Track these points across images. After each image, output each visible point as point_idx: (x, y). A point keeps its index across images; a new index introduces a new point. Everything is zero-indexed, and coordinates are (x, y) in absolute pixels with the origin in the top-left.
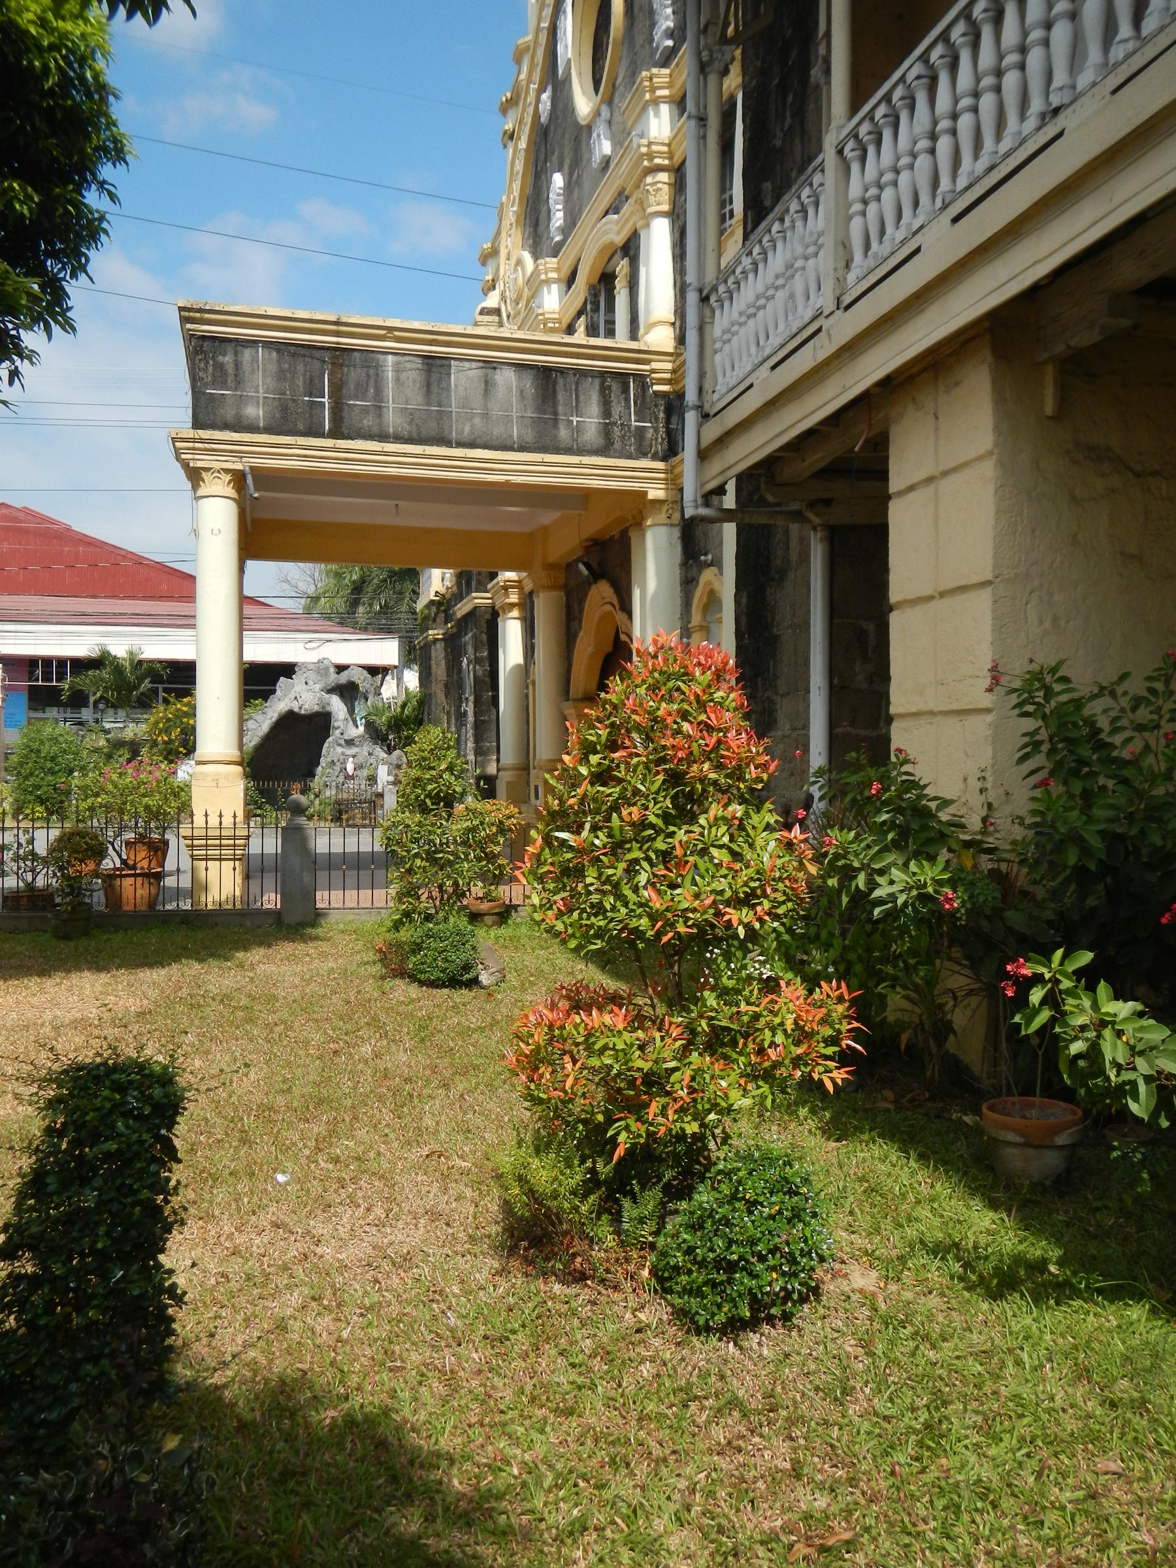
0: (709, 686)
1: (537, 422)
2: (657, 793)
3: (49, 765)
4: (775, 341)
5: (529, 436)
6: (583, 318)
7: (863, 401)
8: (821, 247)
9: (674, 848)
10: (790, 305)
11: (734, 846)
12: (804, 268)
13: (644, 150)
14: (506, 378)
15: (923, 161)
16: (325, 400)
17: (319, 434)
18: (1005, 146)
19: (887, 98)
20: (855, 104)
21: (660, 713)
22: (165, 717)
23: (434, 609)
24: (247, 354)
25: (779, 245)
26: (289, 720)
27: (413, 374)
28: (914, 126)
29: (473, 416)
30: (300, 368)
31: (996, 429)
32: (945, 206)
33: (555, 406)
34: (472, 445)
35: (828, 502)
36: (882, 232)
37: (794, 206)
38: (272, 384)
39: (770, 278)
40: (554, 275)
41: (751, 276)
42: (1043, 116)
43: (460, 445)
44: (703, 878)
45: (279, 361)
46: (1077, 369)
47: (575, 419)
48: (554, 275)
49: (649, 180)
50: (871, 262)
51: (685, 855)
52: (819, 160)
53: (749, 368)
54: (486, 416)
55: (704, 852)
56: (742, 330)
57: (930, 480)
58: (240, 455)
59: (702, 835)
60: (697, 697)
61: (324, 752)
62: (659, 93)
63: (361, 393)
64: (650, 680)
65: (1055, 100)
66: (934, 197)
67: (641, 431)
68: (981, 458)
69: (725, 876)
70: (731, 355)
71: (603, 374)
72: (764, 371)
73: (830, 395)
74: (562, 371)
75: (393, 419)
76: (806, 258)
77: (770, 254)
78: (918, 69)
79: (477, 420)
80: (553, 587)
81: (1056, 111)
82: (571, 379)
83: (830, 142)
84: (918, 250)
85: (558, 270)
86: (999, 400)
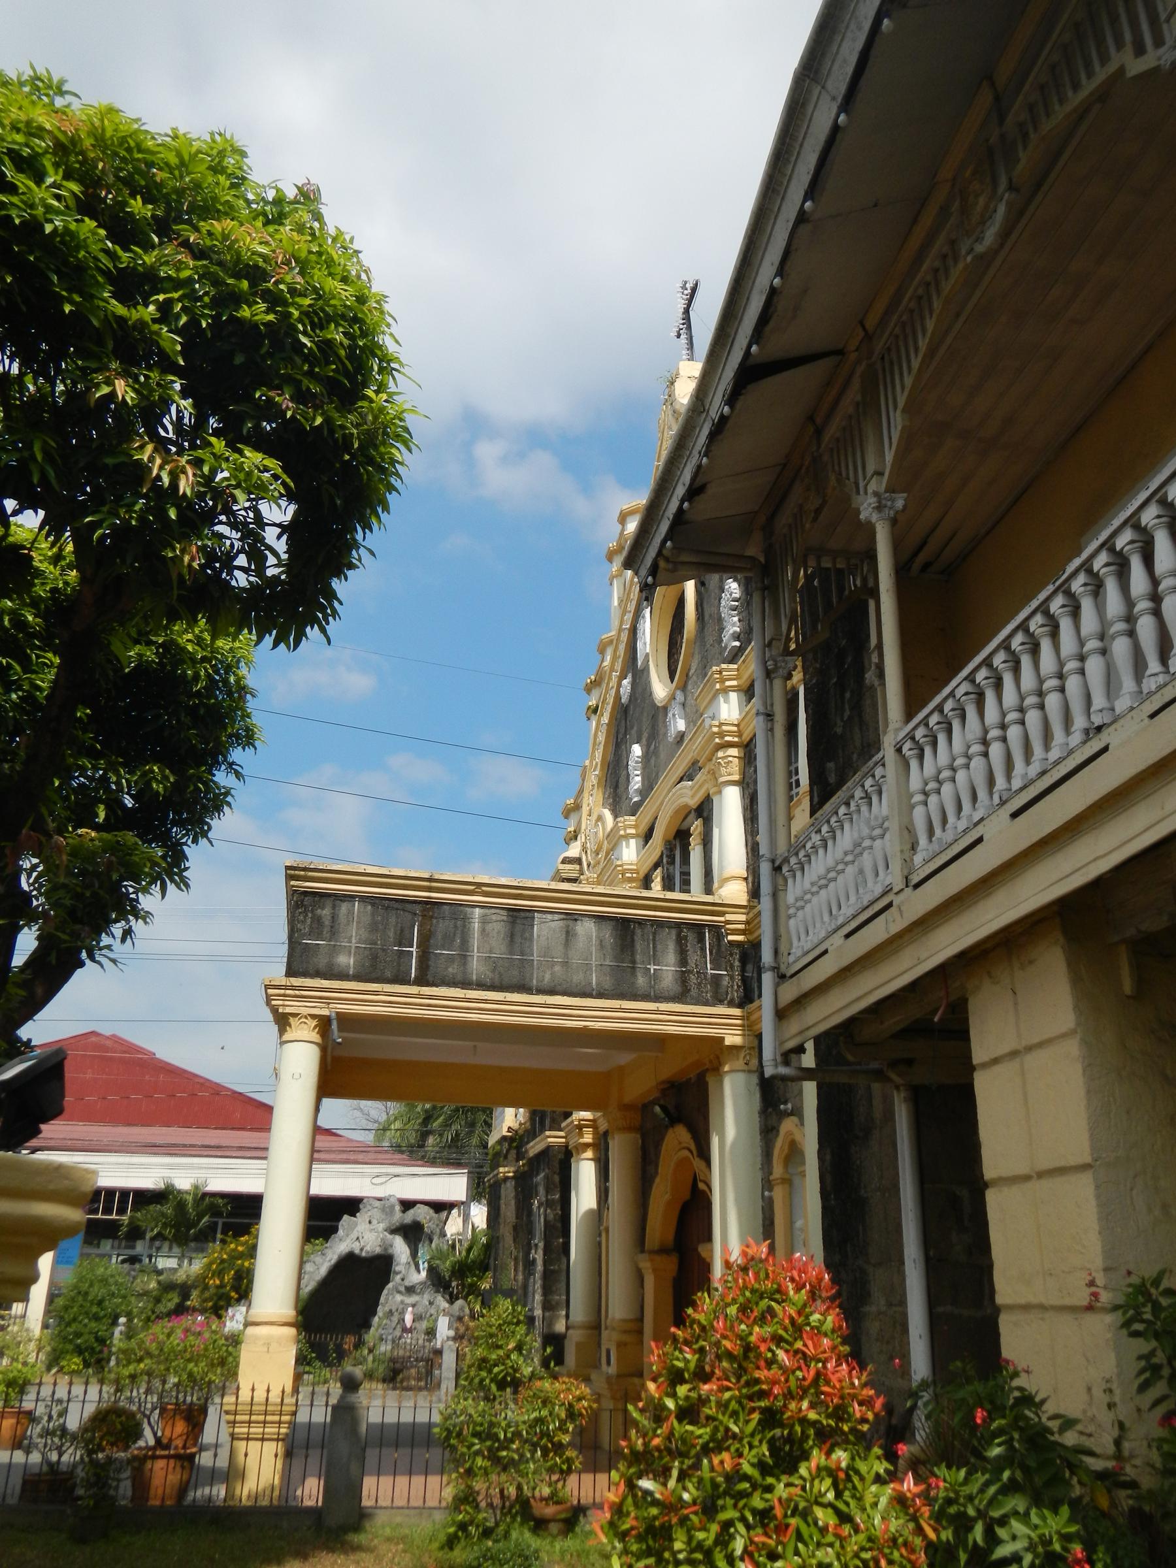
0: (805, 1305)
1: (616, 970)
2: (752, 1435)
3: (95, 1309)
4: (847, 911)
5: (608, 983)
6: (659, 870)
7: (942, 971)
8: (887, 829)
9: (772, 1508)
10: (860, 880)
11: (841, 1505)
12: (871, 847)
13: (715, 729)
14: (587, 928)
15: (977, 763)
16: (414, 949)
17: (405, 981)
18: (1054, 754)
19: (940, 708)
20: (909, 715)
21: (753, 1339)
23: (506, 1145)
24: (344, 907)
25: (847, 826)
26: (349, 1261)
27: (498, 927)
28: (966, 734)
29: (553, 964)
30: (393, 920)
31: (1076, 1007)
32: (1003, 803)
33: (633, 955)
34: (552, 992)
35: (909, 1062)
36: (944, 821)
37: (858, 793)
38: (364, 934)
39: (839, 854)
40: (633, 831)
41: (821, 851)
42: (1087, 731)
43: (540, 992)
44: (806, 1545)
45: (373, 914)
46: (1150, 951)
47: (652, 968)
48: (633, 831)
49: (720, 754)
50: (935, 847)
51: (786, 1516)
52: (880, 755)
53: (823, 934)
54: (565, 964)
55: (805, 1514)
56: (815, 900)
57: (1014, 1054)
58: (327, 1001)
59: (803, 1488)
60: (793, 1322)
61: (382, 1299)
62: (728, 683)
63: (448, 942)
64: (741, 1299)
65: (1097, 720)
66: (991, 793)
67: (716, 979)
68: (1064, 1036)
69: (831, 1545)
70: (804, 920)
71: (679, 926)
72: (838, 939)
73: (906, 964)
74: (641, 922)
75: (476, 967)
76: (873, 839)
77: (838, 833)
78: (965, 687)
79: (557, 968)
80: (629, 1129)
81: (1099, 729)
82: (649, 929)
83: (888, 742)
84: (980, 840)
85: (636, 827)
86: (1076, 980)
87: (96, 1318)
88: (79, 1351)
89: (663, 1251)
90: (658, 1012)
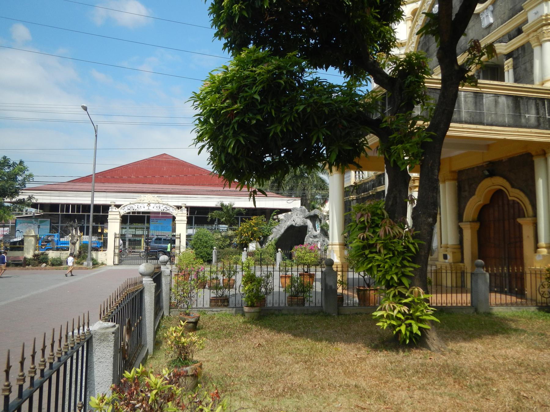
1: (514, 116)
3: (205, 244)
5: (512, 122)
13: (544, 18)
14: (502, 100)
22: (246, 227)
23: (352, 188)
27: (470, 99)
33: (520, 110)
34: (492, 125)
43: (488, 125)
47: (527, 115)
49: (545, 28)
54: (496, 114)
61: (305, 240)
71: (536, 99)
74: (521, 97)
79: (493, 116)
82: (525, 100)
87: (205, 247)
88: (202, 257)
89: (473, 221)
90: (531, 132)
